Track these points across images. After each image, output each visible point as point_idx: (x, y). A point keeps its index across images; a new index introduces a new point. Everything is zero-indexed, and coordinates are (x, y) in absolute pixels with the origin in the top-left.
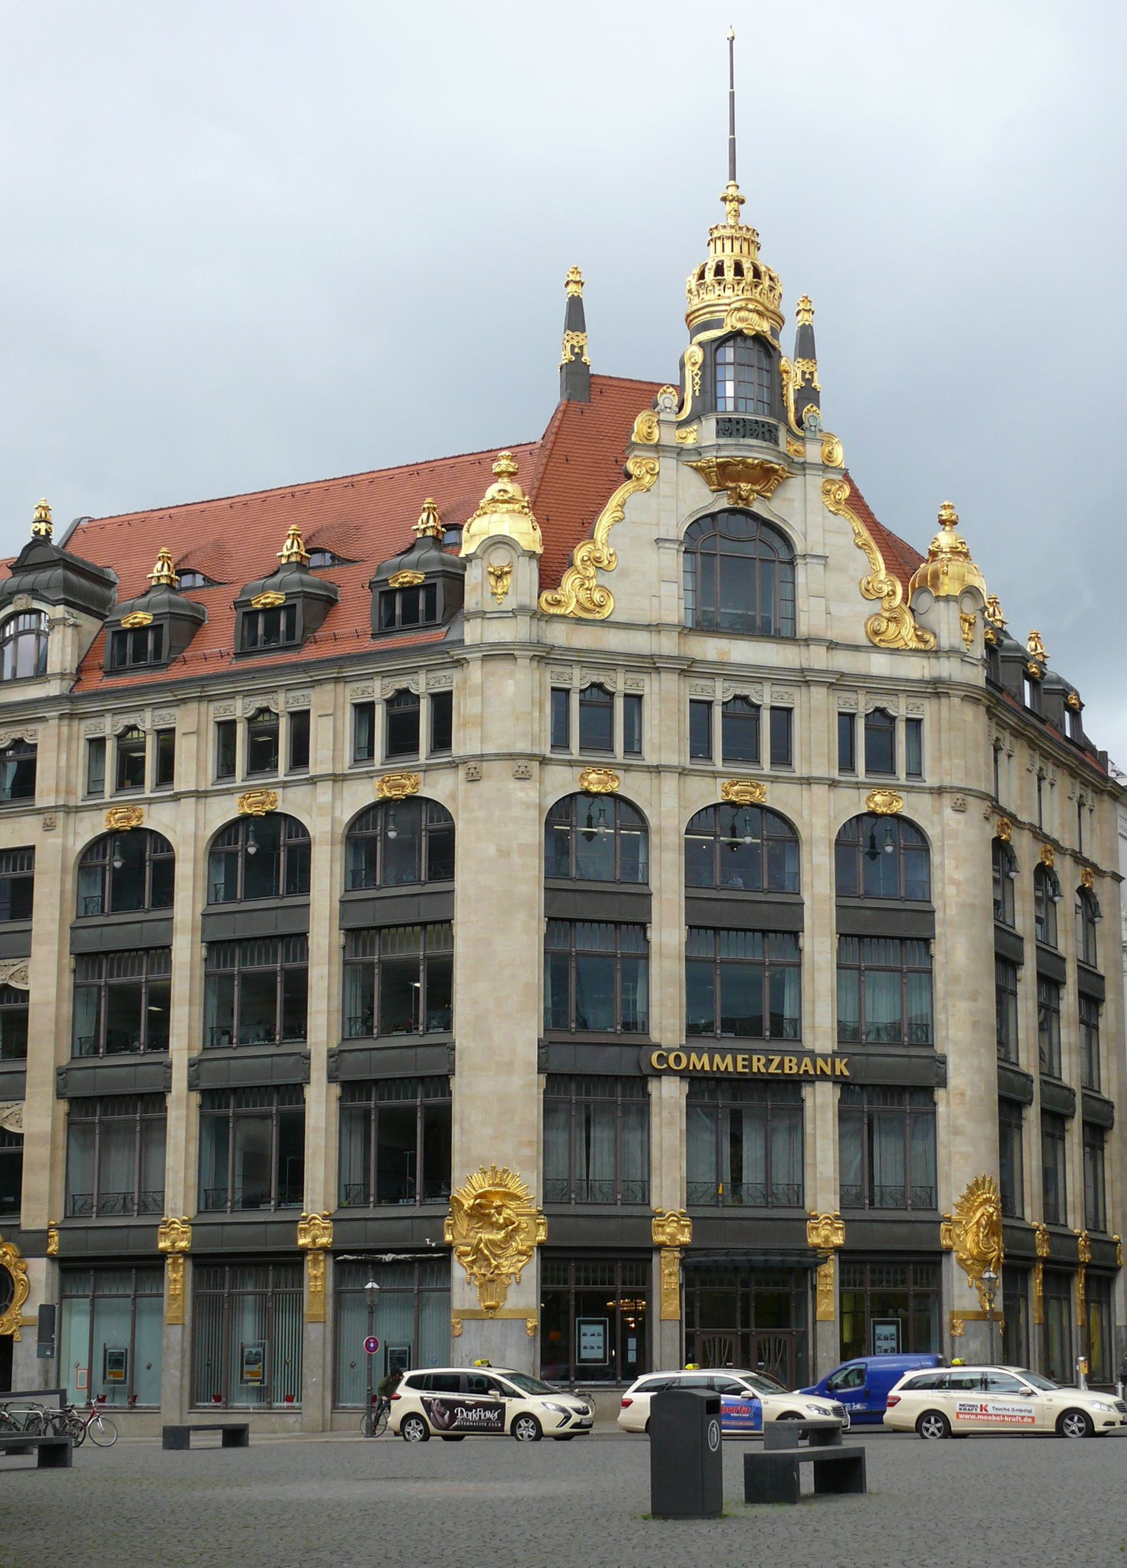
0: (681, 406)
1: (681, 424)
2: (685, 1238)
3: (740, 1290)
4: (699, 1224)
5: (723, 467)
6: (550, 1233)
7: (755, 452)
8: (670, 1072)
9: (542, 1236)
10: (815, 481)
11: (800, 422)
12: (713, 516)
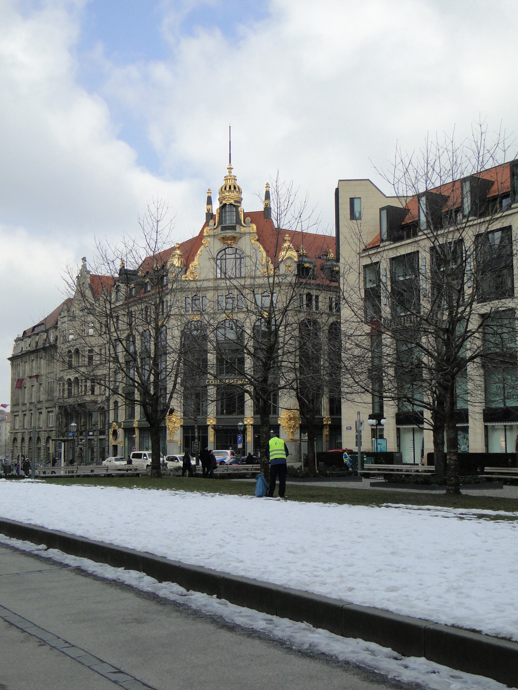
0: (215, 224)
1: (215, 229)
2: (214, 423)
3: (229, 435)
4: (218, 420)
5: (223, 238)
6: (184, 422)
7: (229, 233)
8: (210, 385)
9: (182, 424)
10: (248, 237)
11: (244, 222)
12: (225, 250)
